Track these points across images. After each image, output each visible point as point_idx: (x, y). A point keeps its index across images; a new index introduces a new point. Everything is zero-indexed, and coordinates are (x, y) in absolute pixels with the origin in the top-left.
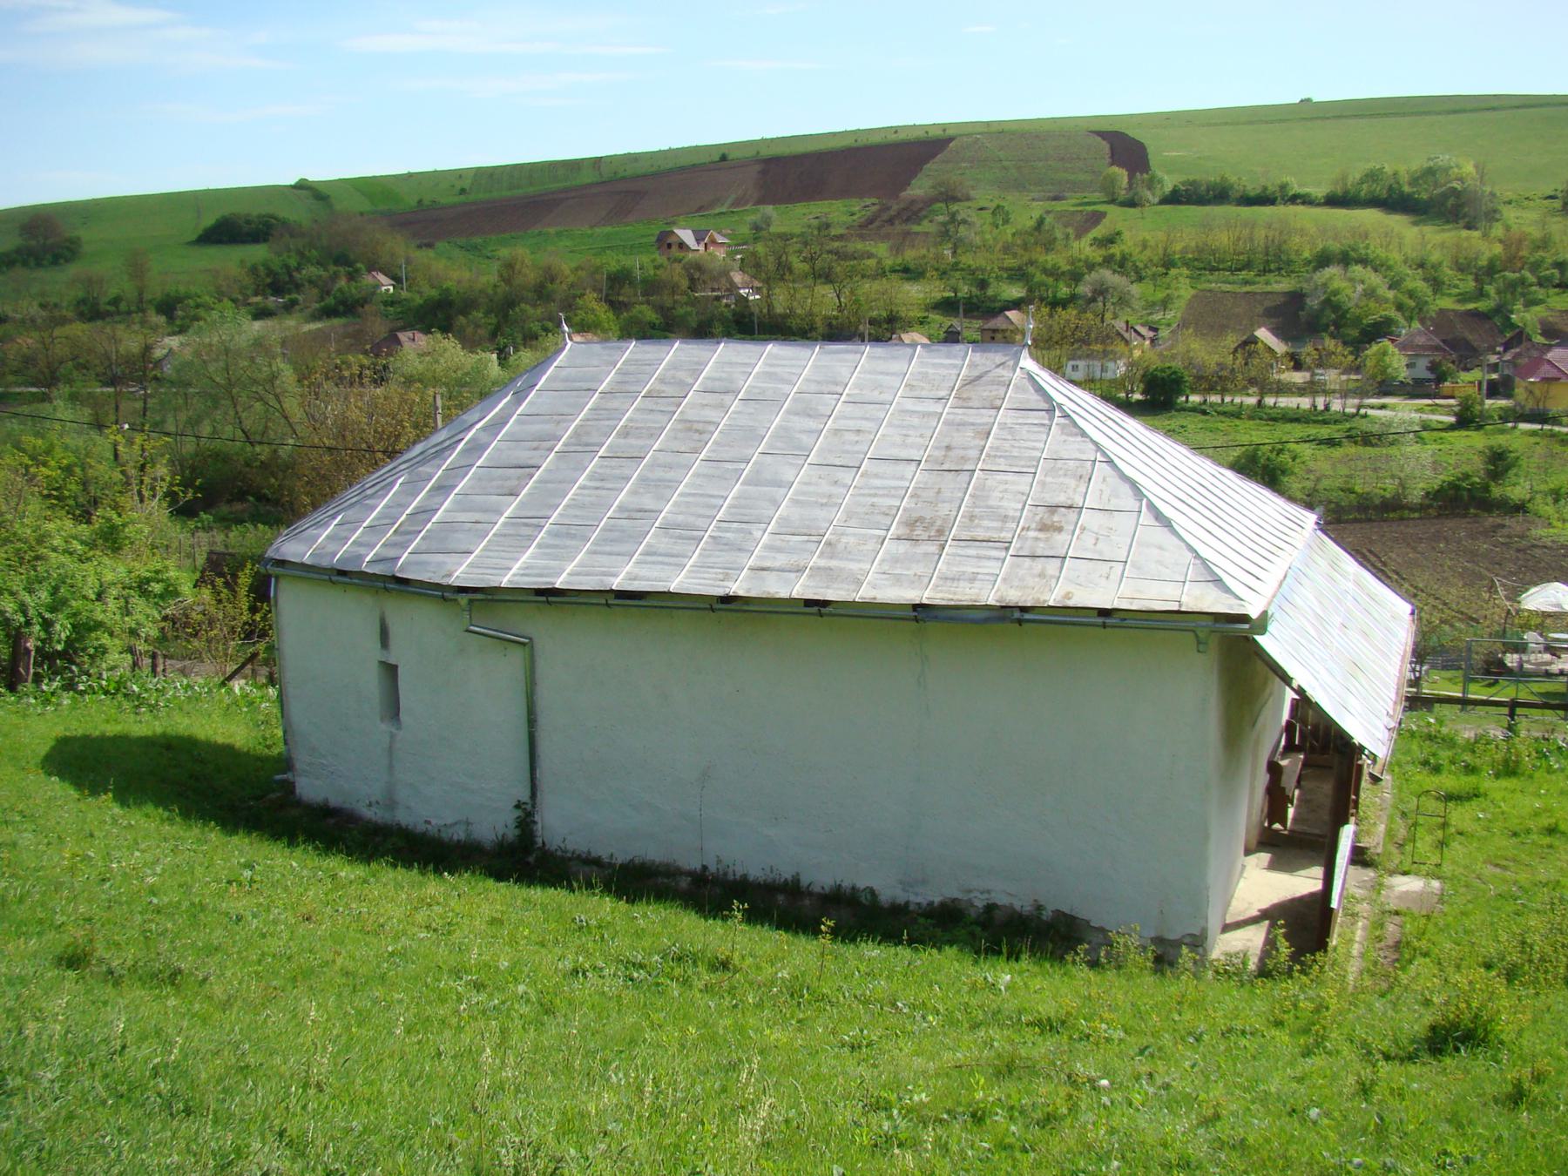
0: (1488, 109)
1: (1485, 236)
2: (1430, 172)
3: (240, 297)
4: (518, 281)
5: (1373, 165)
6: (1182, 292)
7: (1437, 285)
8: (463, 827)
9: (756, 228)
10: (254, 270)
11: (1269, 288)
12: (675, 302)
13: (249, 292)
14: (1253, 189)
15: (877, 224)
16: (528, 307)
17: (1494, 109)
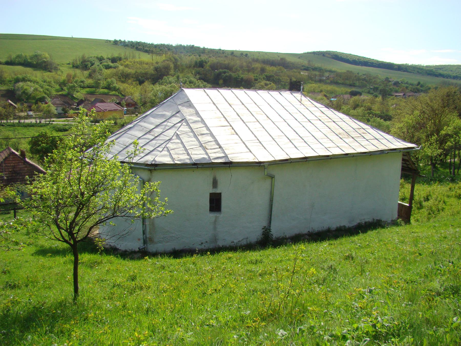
2: (36, 56)
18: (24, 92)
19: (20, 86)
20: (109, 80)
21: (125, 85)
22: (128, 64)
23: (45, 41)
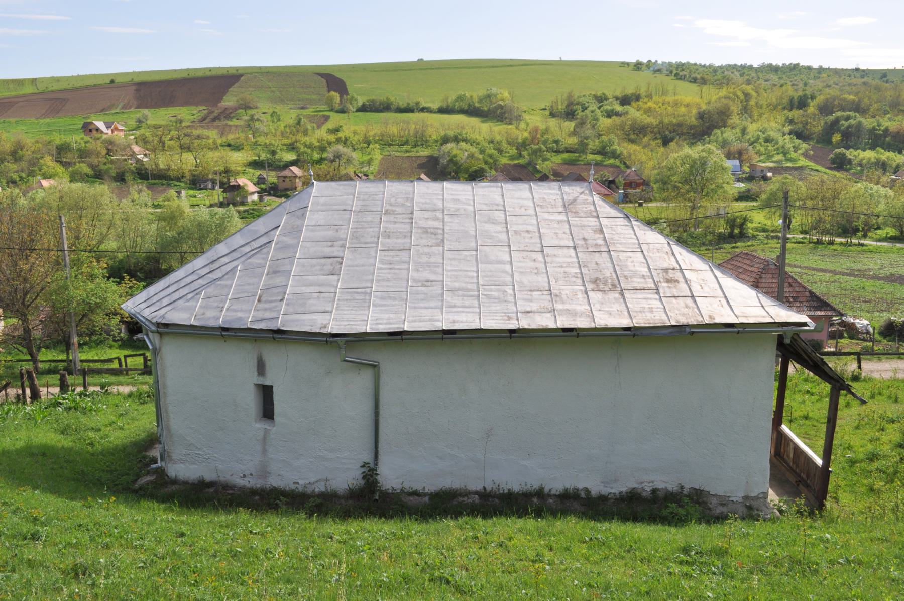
0: (508, 66)
1: (517, 127)
2: (489, 96)
5: (461, 93)
6: (377, 156)
7: (500, 151)
8: (323, 484)
9: (139, 121)
11: (418, 154)
12: (99, 162)
14: (403, 104)
15: (207, 121)
17: (511, 66)
18: (451, 160)
19: (447, 150)
20: (605, 138)
21: (633, 147)
22: (650, 108)
23: (511, 69)
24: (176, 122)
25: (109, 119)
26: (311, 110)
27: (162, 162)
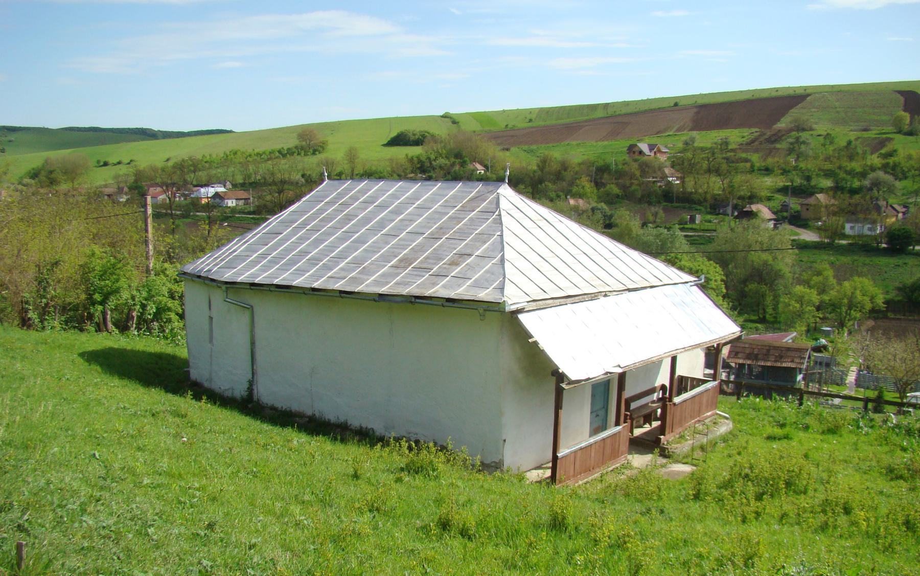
3: (403, 174)
4: (547, 169)
9: (686, 143)
10: (411, 160)
13: (407, 171)
16: (550, 184)
24: (721, 145)
25: (653, 141)
26: (874, 132)
27: (690, 186)
